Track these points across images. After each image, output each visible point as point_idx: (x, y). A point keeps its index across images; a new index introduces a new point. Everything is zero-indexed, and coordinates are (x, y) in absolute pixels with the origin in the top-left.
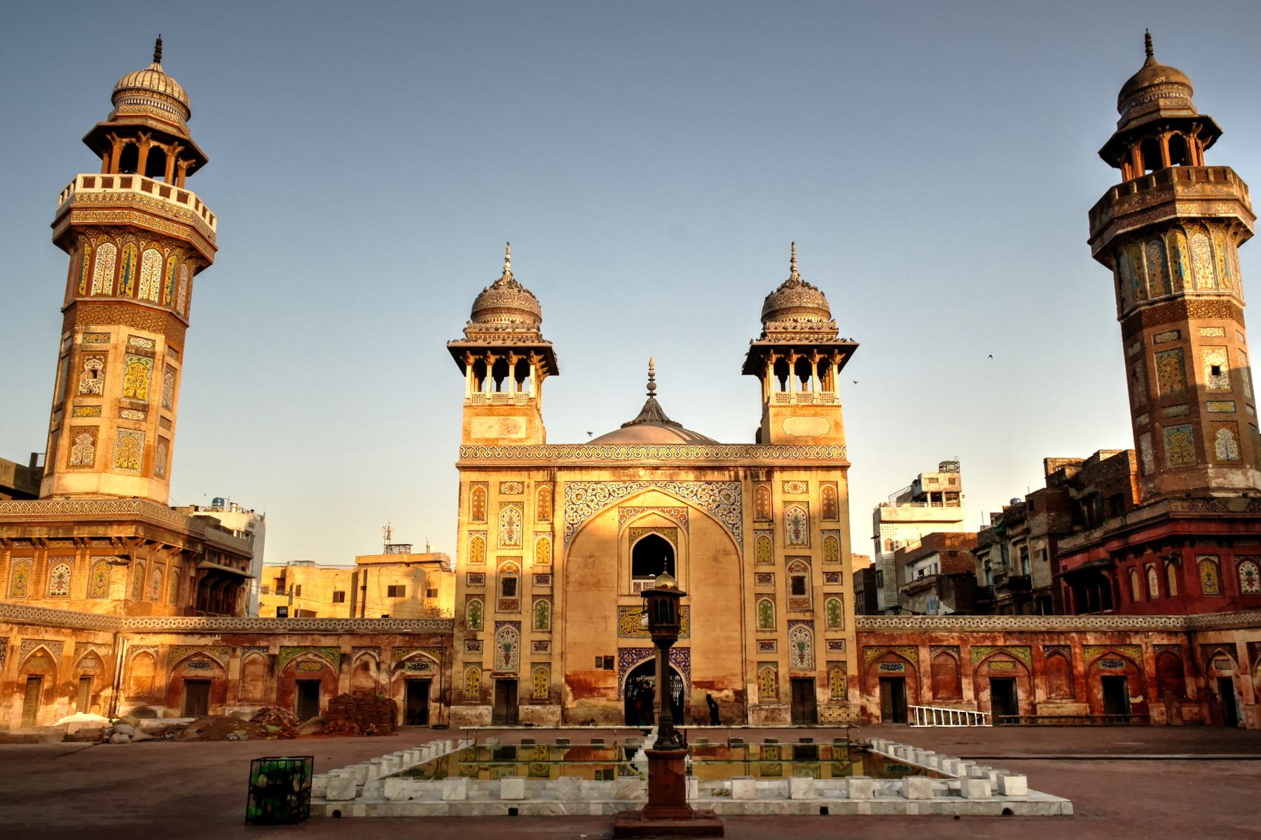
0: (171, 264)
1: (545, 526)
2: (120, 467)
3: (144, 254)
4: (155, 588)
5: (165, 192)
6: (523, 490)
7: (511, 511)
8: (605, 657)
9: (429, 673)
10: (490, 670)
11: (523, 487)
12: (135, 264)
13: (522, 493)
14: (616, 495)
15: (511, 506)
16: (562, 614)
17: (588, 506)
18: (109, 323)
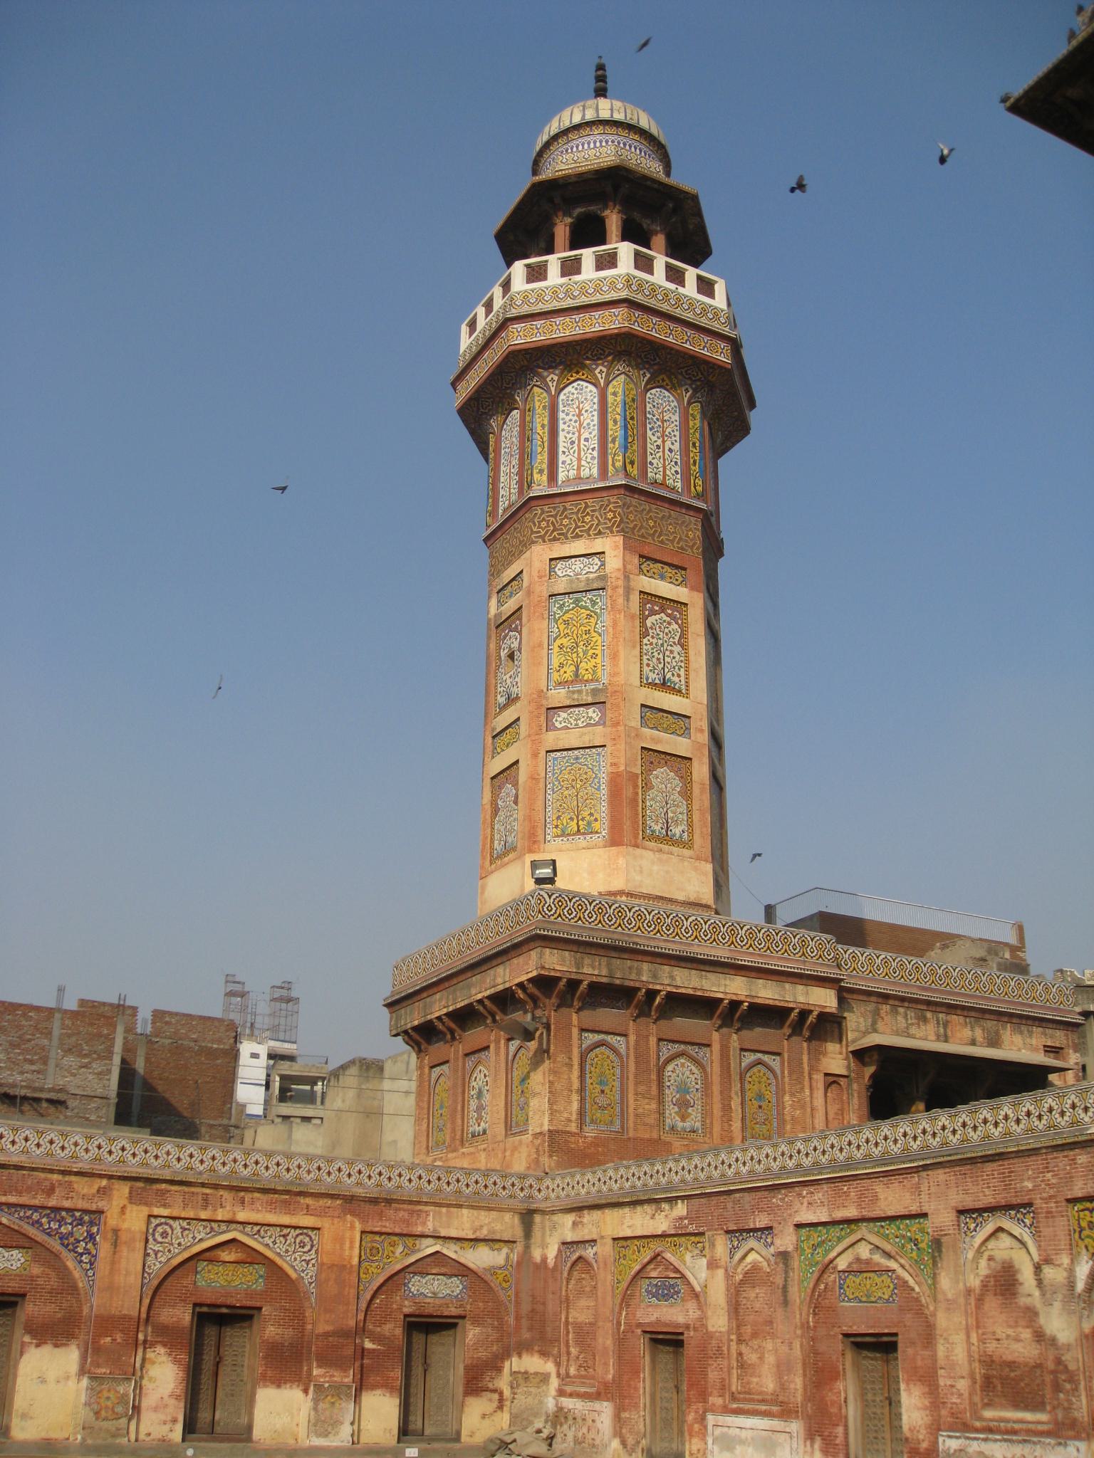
0: (615, 394)
2: (562, 836)
3: (562, 397)
4: (683, 1105)
5: (571, 267)
12: (546, 422)
18: (521, 553)
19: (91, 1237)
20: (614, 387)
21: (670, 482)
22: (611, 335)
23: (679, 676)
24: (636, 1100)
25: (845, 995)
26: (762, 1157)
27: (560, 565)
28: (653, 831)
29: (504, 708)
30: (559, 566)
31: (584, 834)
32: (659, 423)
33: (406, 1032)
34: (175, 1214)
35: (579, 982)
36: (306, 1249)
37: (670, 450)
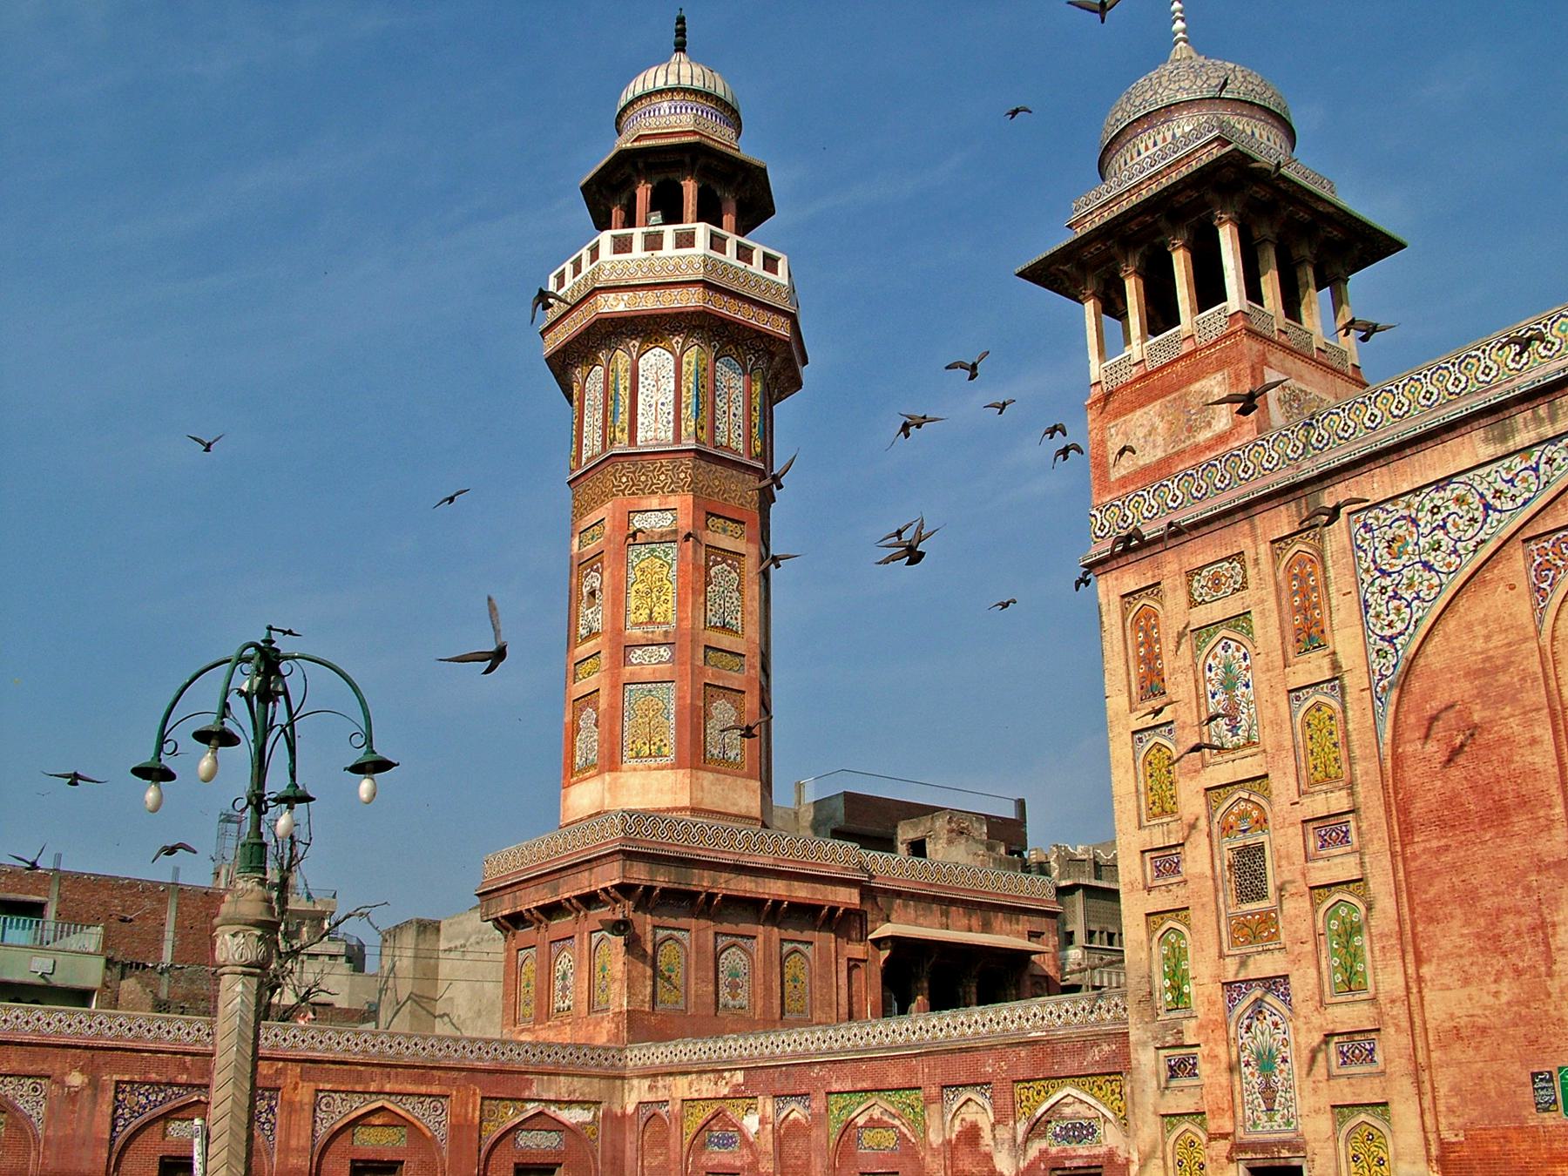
0: (689, 363)
1: (1314, 667)
4: (734, 987)
5: (653, 242)
6: (1244, 577)
7: (1226, 648)
8: (1560, 1069)
9: (1096, 1151)
10: (1225, 1136)
11: (1243, 567)
12: (627, 385)
13: (1244, 586)
14: (1510, 505)
15: (1223, 632)
16: (1401, 933)
17: (1428, 566)
19: (271, 1109)
20: (688, 357)
21: (733, 445)
22: (688, 313)
23: (736, 619)
24: (696, 984)
25: (868, 892)
26: (803, 1041)
27: (638, 517)
28: (713, 755)
29: (586, 639)
30: (637, 518)
31: (655, 757)
32: (726, 390)
33: (496, 920)
34: (335, 1088)
35: (654, 888)
36: (438, 1113)
37: (735, 415)
